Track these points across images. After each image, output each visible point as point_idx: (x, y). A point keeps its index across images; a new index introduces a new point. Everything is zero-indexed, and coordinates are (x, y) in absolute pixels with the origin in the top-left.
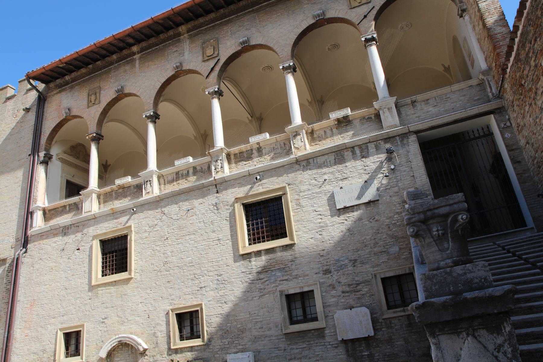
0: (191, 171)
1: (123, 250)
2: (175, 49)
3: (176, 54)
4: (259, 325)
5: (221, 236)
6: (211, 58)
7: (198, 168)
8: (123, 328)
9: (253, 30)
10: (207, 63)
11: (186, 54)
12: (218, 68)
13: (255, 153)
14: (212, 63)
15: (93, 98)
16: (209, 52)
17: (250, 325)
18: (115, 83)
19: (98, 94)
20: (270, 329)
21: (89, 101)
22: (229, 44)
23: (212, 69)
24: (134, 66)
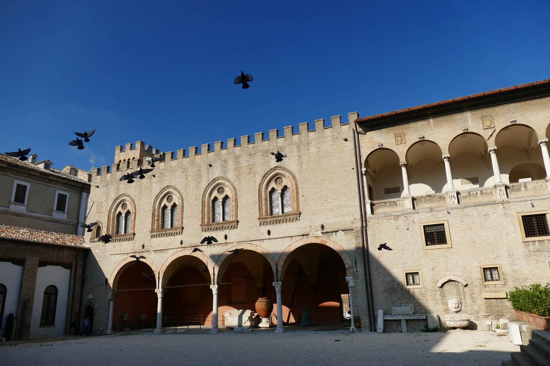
0: (479, 192)
1: (442, 232)
2: (460, 117)
3: (461, 120)
4: (536, 277)
5: (508, 232)
6: (489, 128)
7: (484, 191)
8: (448, 273)
9: (518, 114)
10: (486, 130)
11: (470, 122)
12: (495, 135)
13: (523, 188)
14: (490, 132)
15: (399, 139)
16: (488, 123)
17: (531, 277)
18: (415, 131)
19: (403, 138)
20: (543, 279)
21: (397, 141)
22: (501, 120)
23: (491, 135)
24: (430, 123)
